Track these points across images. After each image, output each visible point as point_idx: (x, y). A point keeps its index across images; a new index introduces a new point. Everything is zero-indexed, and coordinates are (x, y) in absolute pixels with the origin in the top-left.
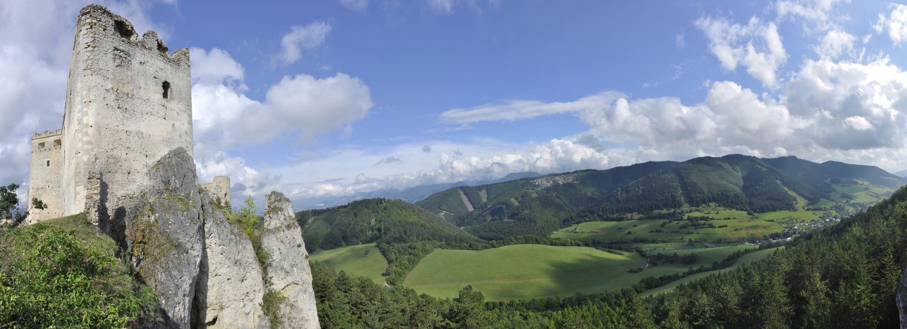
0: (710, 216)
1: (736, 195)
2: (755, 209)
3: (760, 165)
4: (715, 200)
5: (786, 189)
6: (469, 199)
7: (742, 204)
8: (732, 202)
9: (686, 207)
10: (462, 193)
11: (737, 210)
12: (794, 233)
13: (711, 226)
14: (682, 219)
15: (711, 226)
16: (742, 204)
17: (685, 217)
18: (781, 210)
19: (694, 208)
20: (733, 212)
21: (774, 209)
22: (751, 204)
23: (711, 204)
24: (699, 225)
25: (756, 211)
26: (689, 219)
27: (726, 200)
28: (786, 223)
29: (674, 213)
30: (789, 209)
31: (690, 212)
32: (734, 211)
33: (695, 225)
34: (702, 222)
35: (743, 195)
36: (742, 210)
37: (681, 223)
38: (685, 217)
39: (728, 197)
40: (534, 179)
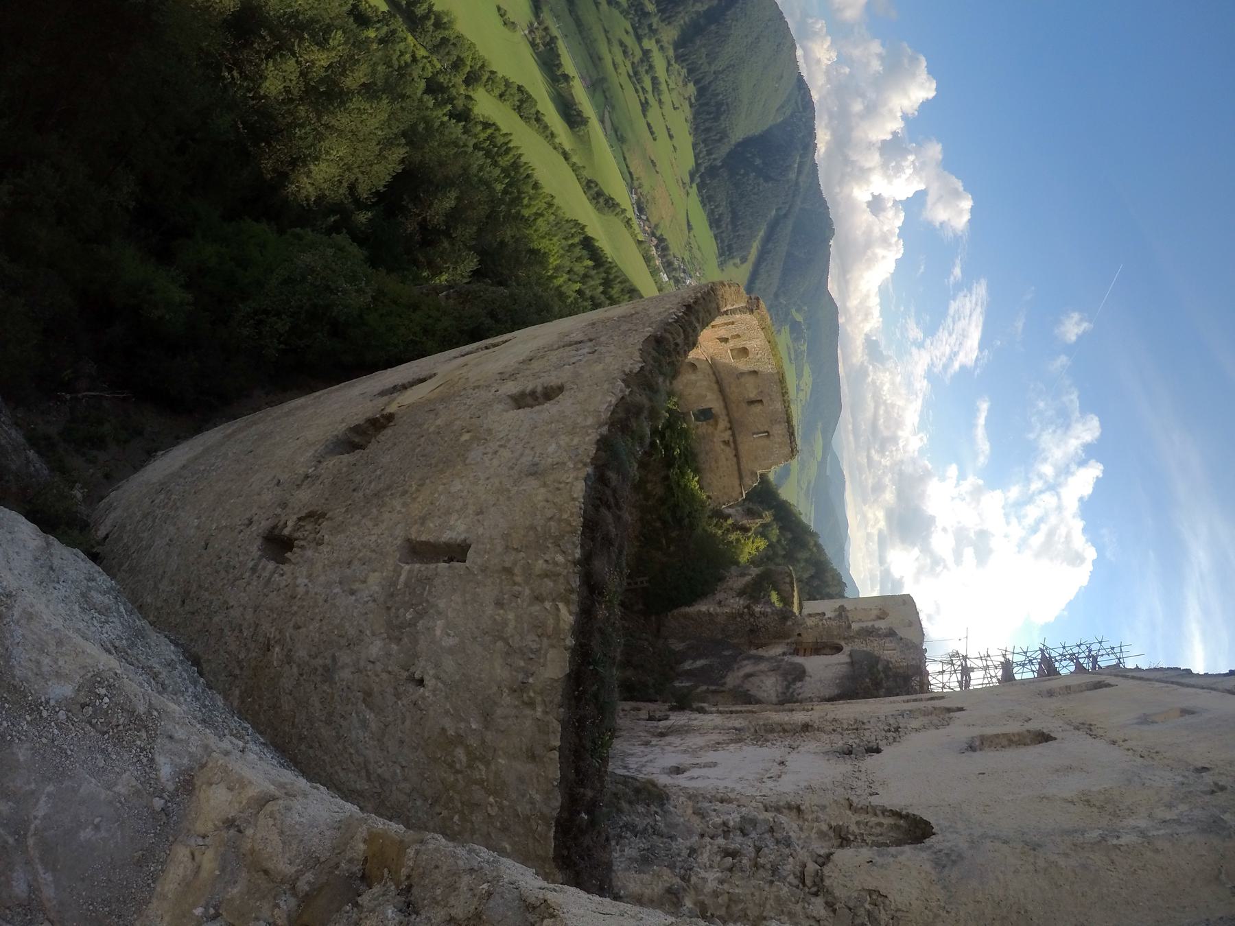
0: (666, 97)
1: (723, 136)
2: (705, 177)
3: (800, 166)
4: (701, 92)
5: (762, 233)
7: (709, 153)
8: (708, 130)
9: (670, 34)
11: (695, 146)
12: (677, 281)
13: (645, 106)
14: (639, 39)
15: (645, 106)
16: (709, 153)
17: (648, 44)
18: (716, 237)
19: (671, 53)
20: (685, 139)
21: (714, 222)
22: (712, 171)
23: (691, 85)
24: (640, 81)
25: (700, 187)
26: (646, 53)
27: (709, 112)
28: (693, 257)
29: (646, 15)
30: (720, 255)
31: (662, 48)
32: (690, 139)
33: (636, 73)
34: (647, 83)
35: (724, 150)
36: (696, 157)
37: (630, 41)
38: (648, 44)
39: (716, 119)
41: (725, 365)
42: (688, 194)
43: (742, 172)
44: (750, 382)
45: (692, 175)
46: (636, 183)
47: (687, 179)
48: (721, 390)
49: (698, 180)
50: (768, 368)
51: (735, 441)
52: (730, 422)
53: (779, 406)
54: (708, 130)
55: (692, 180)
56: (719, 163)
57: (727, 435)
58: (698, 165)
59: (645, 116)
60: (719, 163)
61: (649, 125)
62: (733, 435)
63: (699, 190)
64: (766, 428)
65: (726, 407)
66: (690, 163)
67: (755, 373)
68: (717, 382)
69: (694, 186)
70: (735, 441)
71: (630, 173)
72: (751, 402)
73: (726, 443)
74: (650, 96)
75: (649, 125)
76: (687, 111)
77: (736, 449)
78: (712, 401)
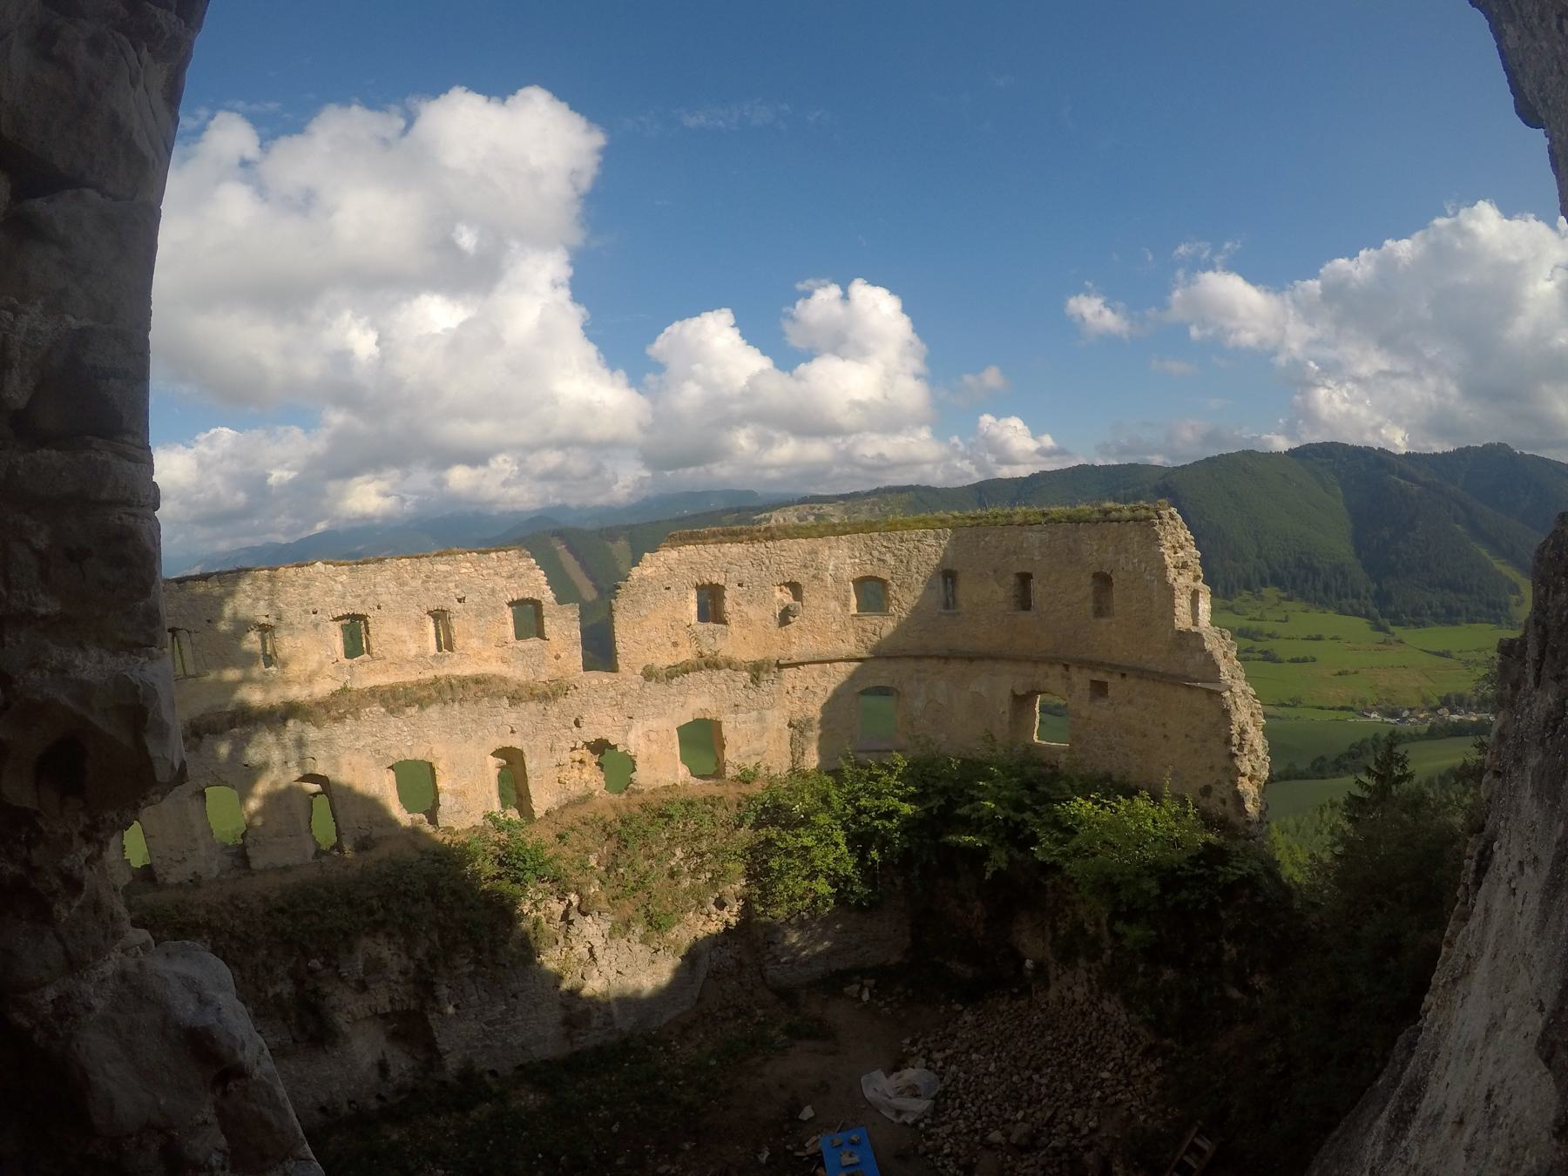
6: (584, 566)
7: (1357, 596)
10: (561, 548)
22: (1382, 598)
36: (1356, 614)
40: (760, 510)
41: (901, 629)
42: (1401, 642)
43: (1393, 557)
44: (967, 591)
45: (1379, 628)
46: (1358, 706)
47: (1381, 636)
48: (971, 658)
49: (1386, 622)
50: (930, 548)
51: (1094, 665)
52: (1052, 662)
53: (1033, 537)
54: (1327, 588)
55: (1384, 629)
56: (1374, 587)
57: (1082, 679)
58: (1367, 616)
59: (1280, 661)
60: (1374, 587)
61: (1293, 661)
62: (1083, 664)
63: (1401, 624)
64: (1086, 579)
65: (1015, 659)
66: (1361, 623)
67: (947, 576)
68: (947, 657)
69: (1392, 629)
70: (1094, 665)
71: (1342, 709)
72: (1024, 603)
73: (1099, 689)
74: (1259, 646)
75: (1293, 661)
76: (1295, 606)
77: (1112, 668)
78: (998, 685)
